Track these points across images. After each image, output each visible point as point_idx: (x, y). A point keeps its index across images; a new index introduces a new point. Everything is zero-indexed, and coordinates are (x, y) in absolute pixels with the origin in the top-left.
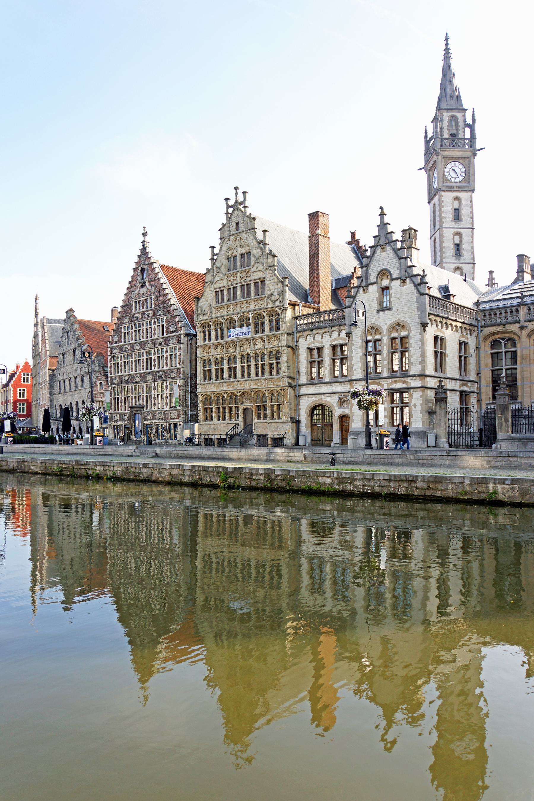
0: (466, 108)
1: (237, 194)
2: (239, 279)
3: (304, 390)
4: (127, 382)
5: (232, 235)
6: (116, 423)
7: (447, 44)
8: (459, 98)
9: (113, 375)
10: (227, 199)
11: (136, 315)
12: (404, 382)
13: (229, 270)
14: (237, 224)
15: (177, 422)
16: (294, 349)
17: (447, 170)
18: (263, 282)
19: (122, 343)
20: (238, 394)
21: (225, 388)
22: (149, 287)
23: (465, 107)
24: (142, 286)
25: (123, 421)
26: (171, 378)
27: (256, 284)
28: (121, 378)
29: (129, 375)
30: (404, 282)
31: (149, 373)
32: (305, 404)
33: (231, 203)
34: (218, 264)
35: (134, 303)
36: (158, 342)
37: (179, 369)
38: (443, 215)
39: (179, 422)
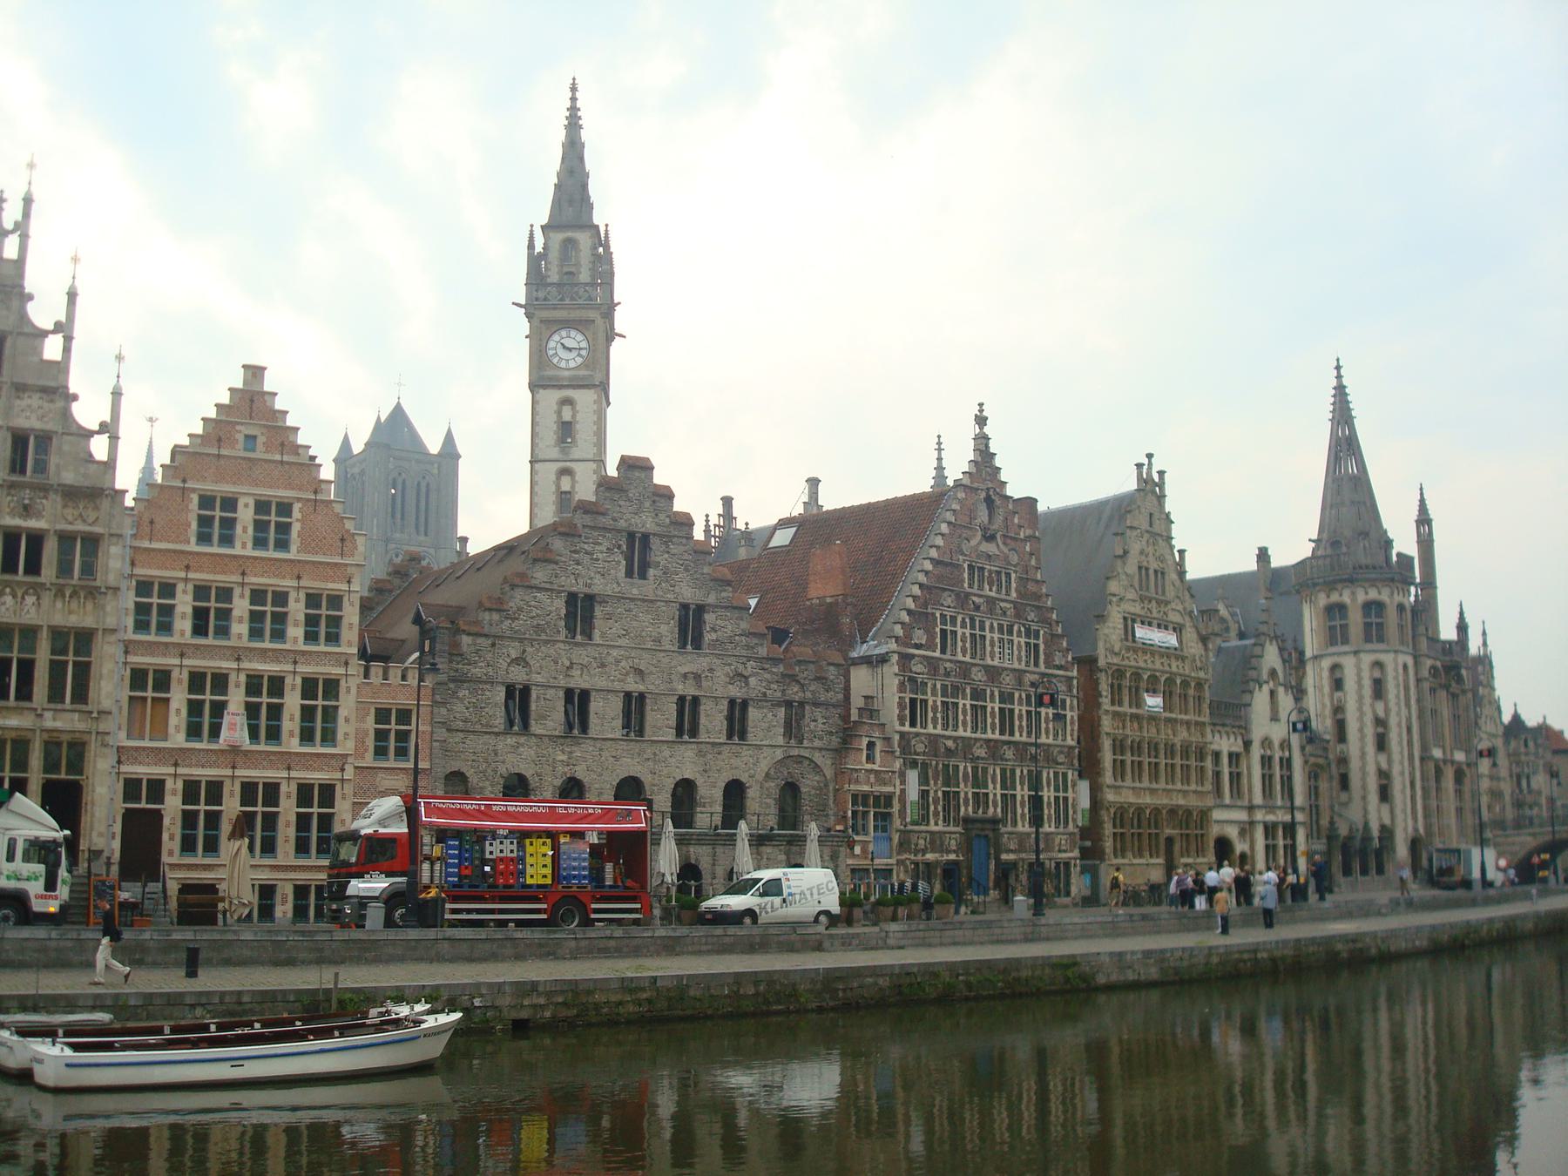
6: (919, 857)
7: (574, 99)
10: (1140, 466)
14: (1151, 515)
15: (1070, 858)
19: (937, 654)
25: (941, 851)
29: (955, 739)
31: (1009, 743)
35: (966, 566)
36: (1029, 678)
37: (1071, 748)
39: (1075, 859)
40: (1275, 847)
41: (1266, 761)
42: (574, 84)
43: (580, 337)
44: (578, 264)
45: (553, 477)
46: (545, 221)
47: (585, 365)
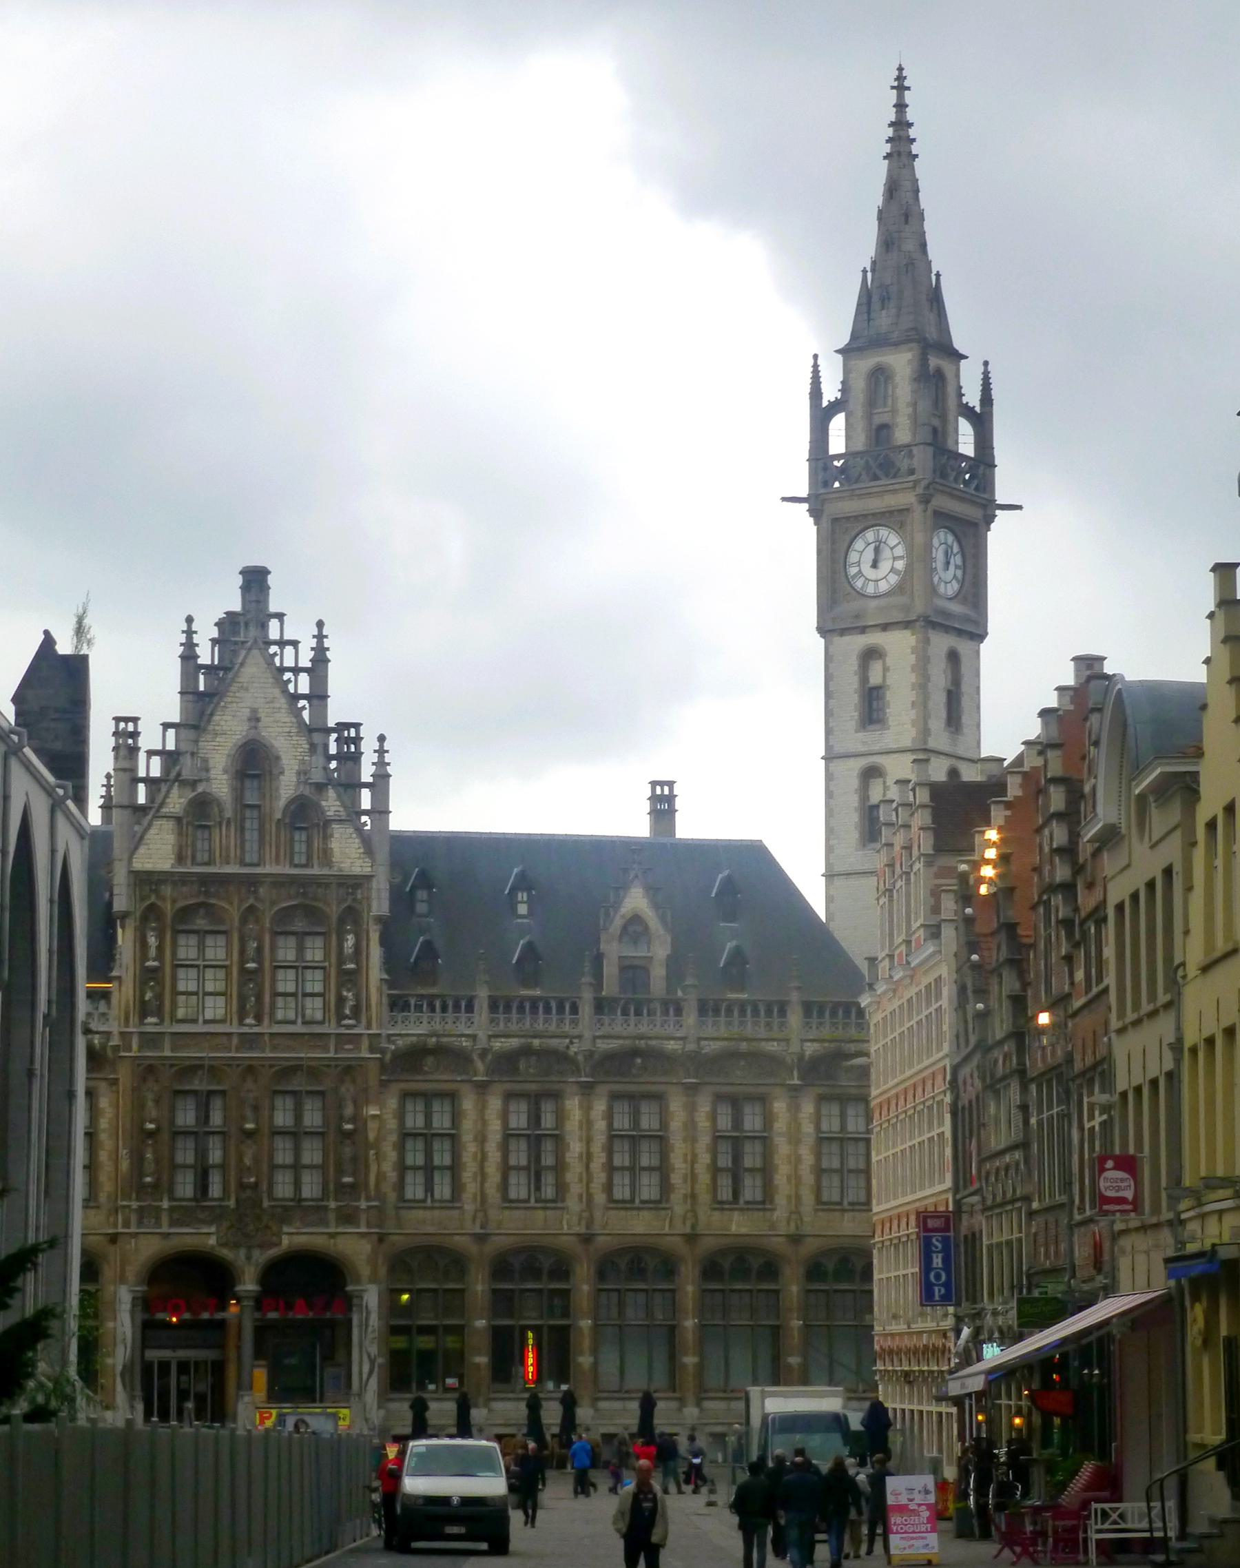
0: (962, 351)
7: (901, 106)
42: (900, 78)
43: (893, 539)
44: (894, 411)
45: (855, 783)
46: (844, 339)
47: (899, 589)
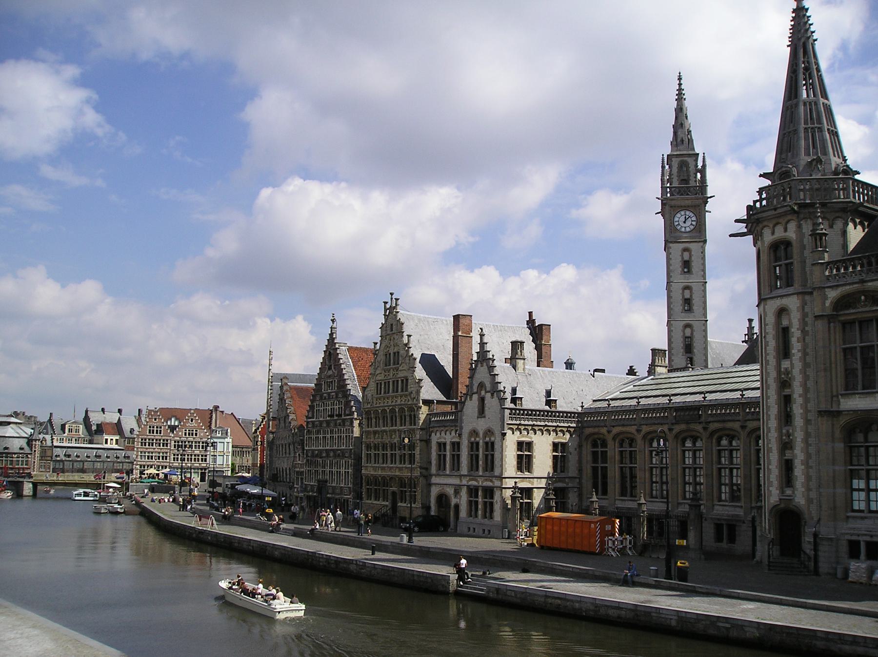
1: (392, 299)
2: (391, 375)
3: (434, 480)
4: (317, 456)
5: (388, 335)
7: (680, 85)
8: (690, 141)
9: (307, 448)
10: (386, 303)
11: (325, 395)
12: (491, 481)
13: (386, 366)
14: (392, 325)
16: (428, 442)
17: (676, 219)
18: (407, 380)
20: (388, 479)
21: (380, 473)
22: (334, 371)
23: (697, 151)
24: (330, 368)
26: (346, 457)
27: (402, 381)
28: (313, 451)
30: (492, 395)
31: (331, 450)
32: (435, 491)
33: (388, 306)
34: (379, 359)
37: (351, 450)
38: (671, 268)
39: (350, 498)
40: (477, 503)
41: (473, 446)
42: (680, 76)
